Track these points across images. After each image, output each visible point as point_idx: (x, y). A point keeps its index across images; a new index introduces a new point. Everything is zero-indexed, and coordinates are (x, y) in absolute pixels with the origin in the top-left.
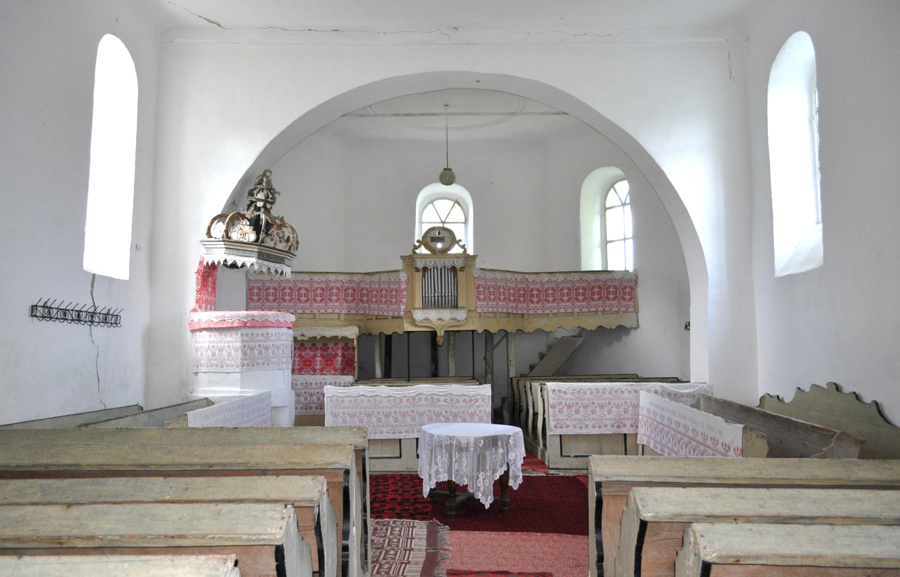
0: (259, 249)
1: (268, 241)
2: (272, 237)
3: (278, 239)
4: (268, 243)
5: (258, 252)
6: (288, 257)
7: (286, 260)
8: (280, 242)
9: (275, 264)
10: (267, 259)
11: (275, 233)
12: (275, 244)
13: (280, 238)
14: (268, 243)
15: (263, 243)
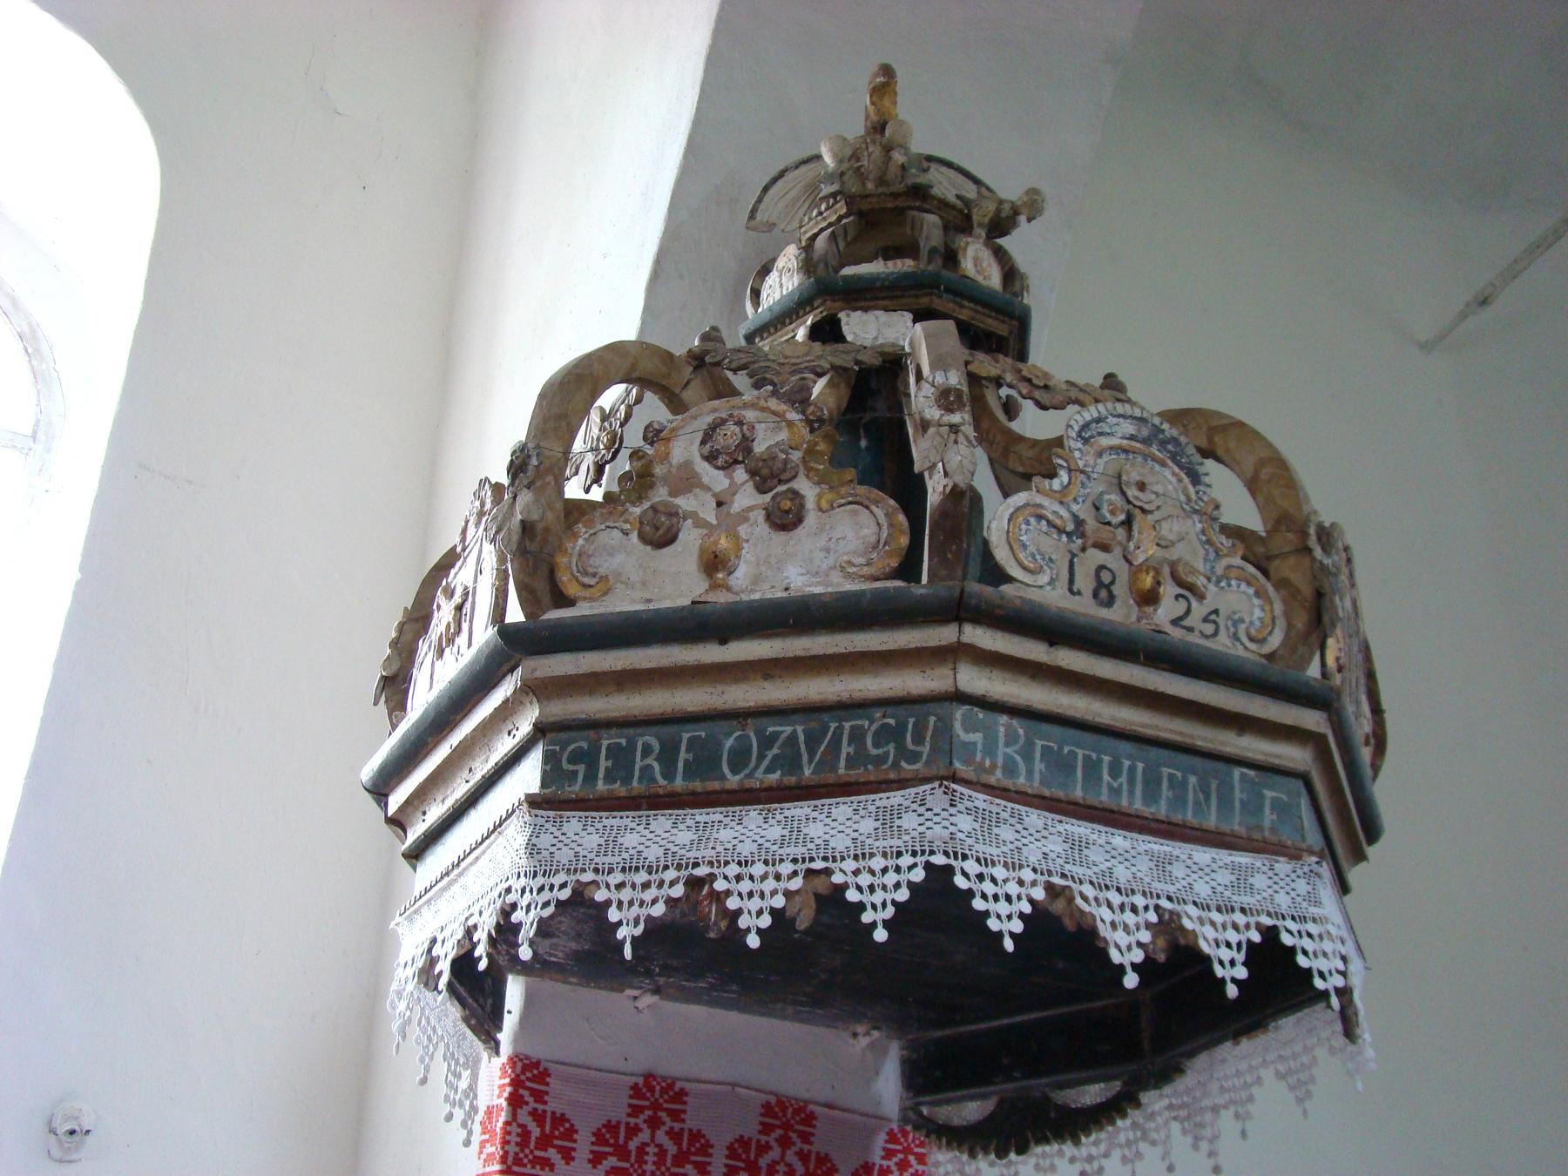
0: (533, 689)
1: (605, 565)
2: (660, 494)
3: (747, 498)
4: (604, 585)
5: (541, 730)
6: (972, 679)
7: (964, 728)
8: (785, 519)
9: (799, 810)
10: (679, 783)
11: (685, 449)
12: (714, 564)
13: (767, 475)
14: (604, 585)
15: (563, 601)
